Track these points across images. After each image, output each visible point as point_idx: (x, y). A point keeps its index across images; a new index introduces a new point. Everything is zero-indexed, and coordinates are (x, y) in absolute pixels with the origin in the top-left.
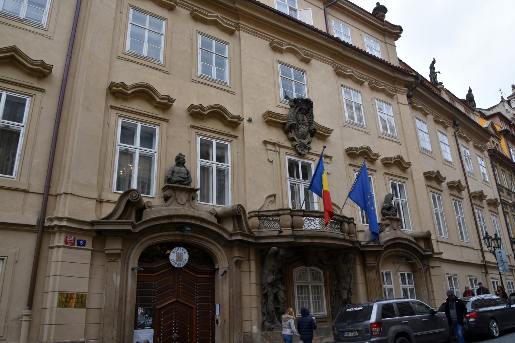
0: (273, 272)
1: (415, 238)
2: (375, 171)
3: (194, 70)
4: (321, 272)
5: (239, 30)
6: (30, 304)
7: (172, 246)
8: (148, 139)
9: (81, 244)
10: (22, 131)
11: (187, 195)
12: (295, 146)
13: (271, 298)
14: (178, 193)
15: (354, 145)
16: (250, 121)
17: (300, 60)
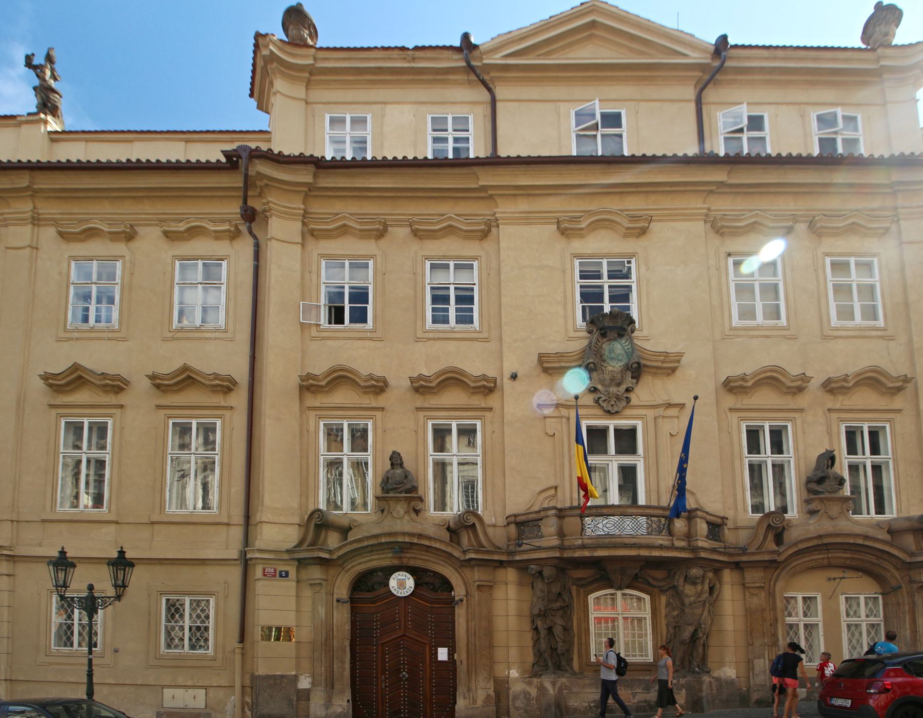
0: (543, 600)
1: (890, 532)
2: (801, 410)
3: (419, 323)
4: (647, 598)
5: (498, 226)
6: (242, 639)
7: (390, 571)
8: (359, 438)
9: (285, 575)
10: (217, 458)
11: (406, 506)
12: (597, 401)
13: (543, 633)
14: (392, 503)
15: (737, 371)
16: (514, 377)
17: (625, 236)
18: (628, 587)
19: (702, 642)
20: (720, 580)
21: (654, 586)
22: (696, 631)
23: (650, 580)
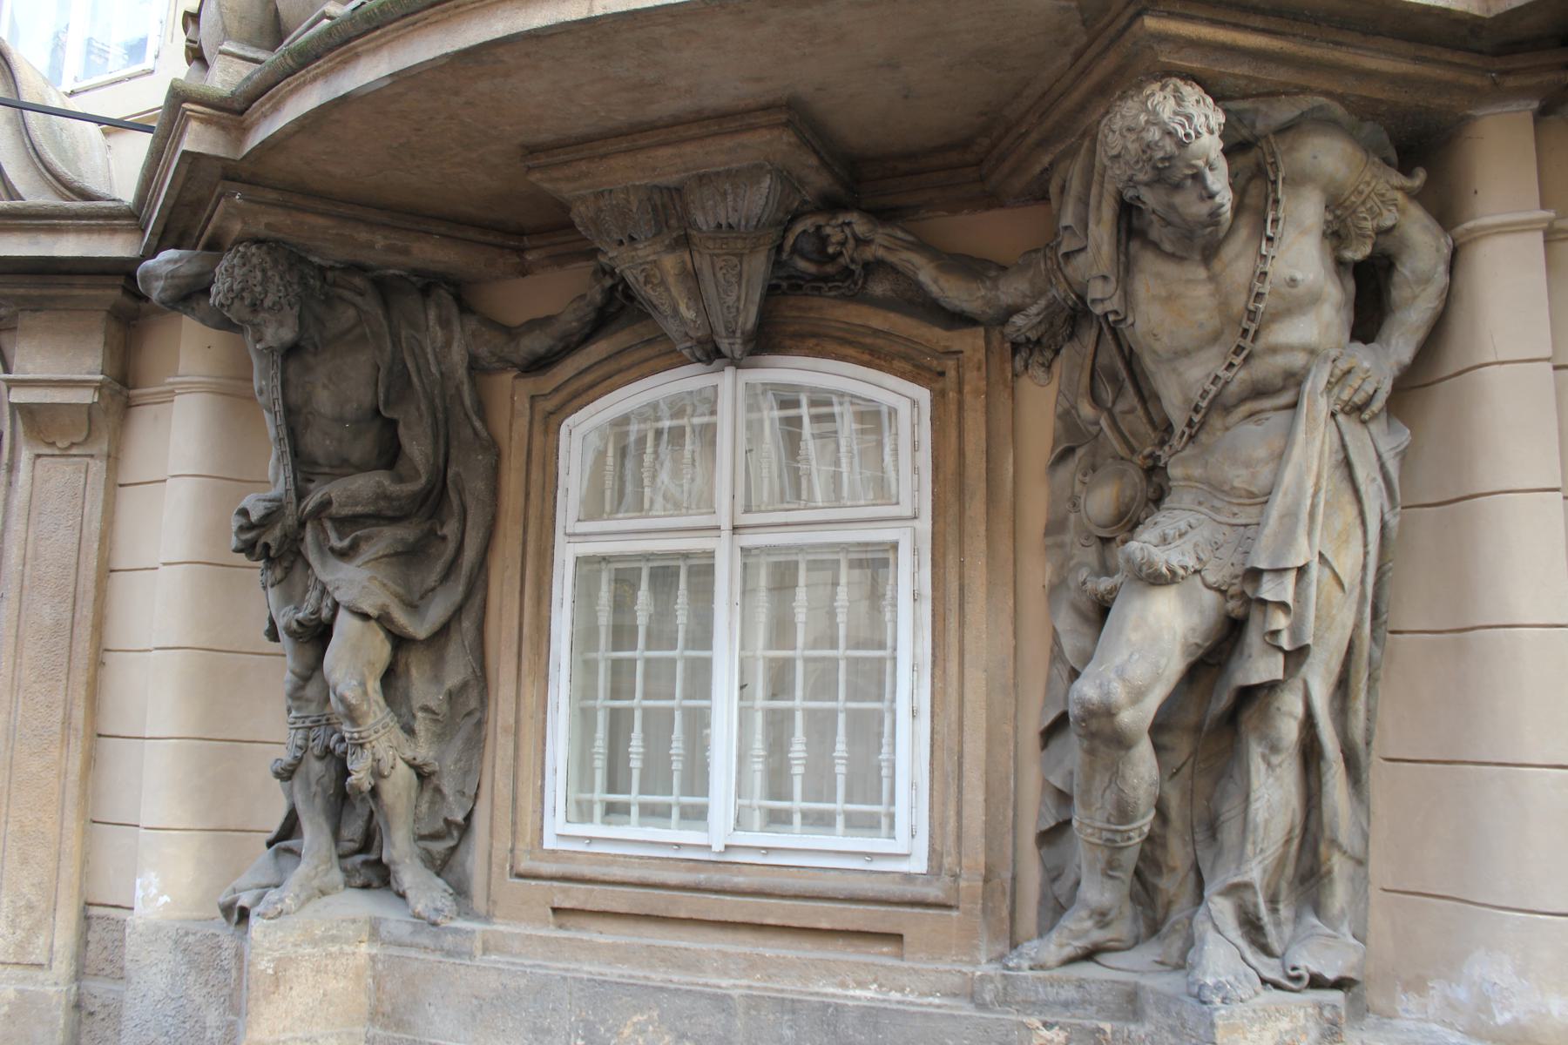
4: (905, 400)
18: (766, 340)
19: (1289, 730)
20: (1444, 207)
21: (958, 319)
22: (1227, 637)
23: (926, 274)
